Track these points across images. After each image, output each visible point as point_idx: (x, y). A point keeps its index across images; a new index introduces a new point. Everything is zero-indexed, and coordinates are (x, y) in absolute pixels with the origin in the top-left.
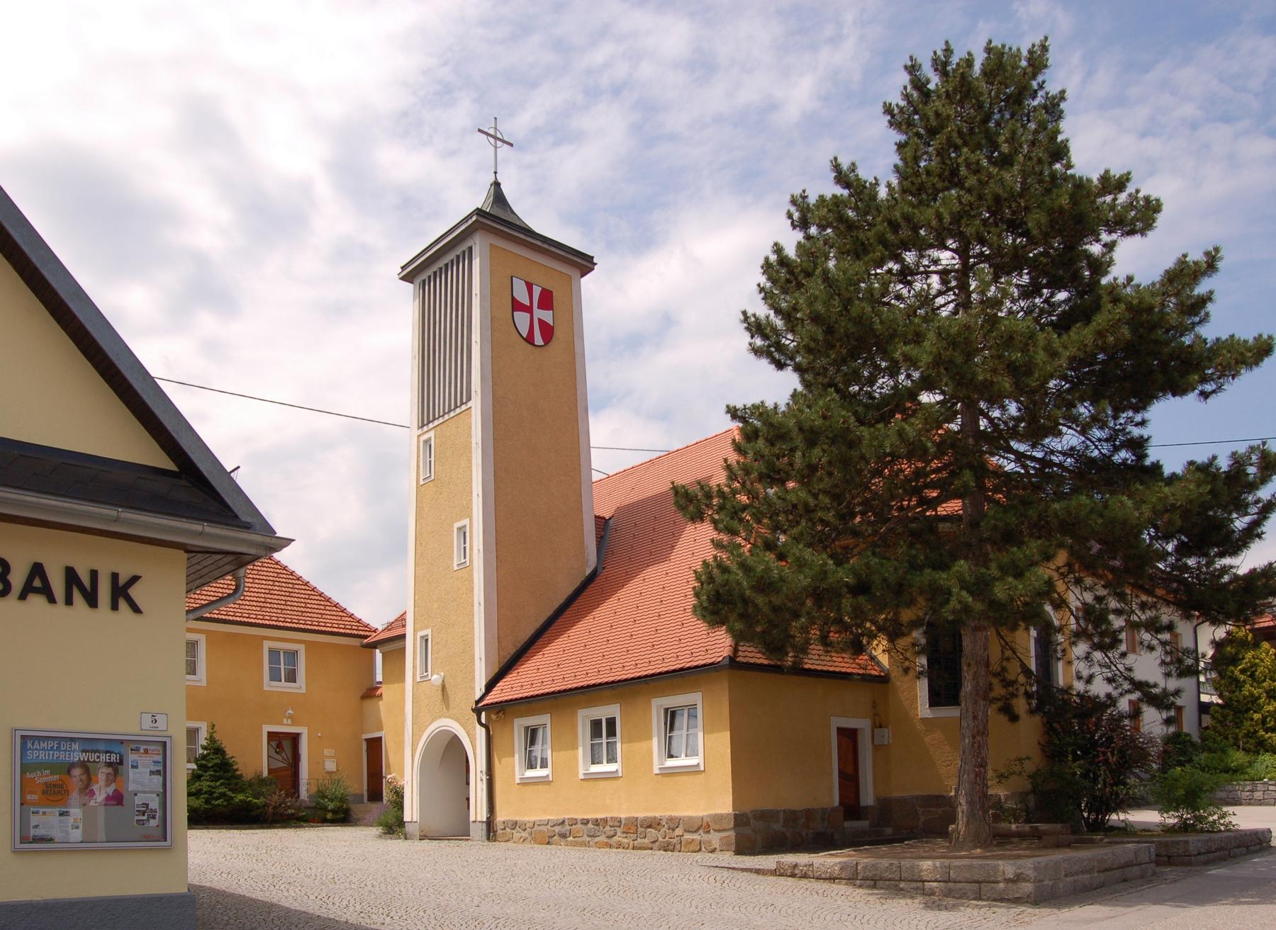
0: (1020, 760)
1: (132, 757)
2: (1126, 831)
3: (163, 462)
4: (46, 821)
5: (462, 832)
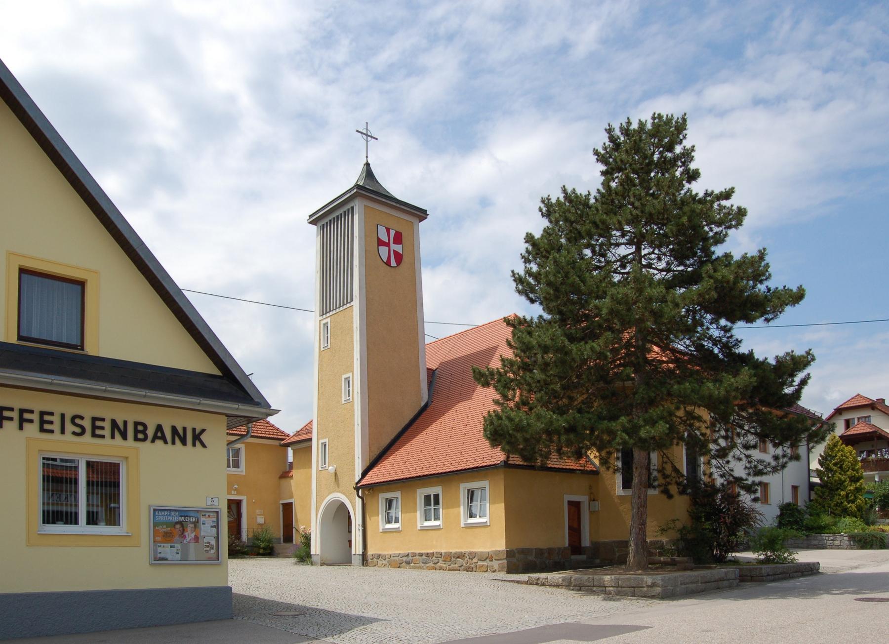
1: (202, 519)
4: (166, 550)
5: (346, 561)
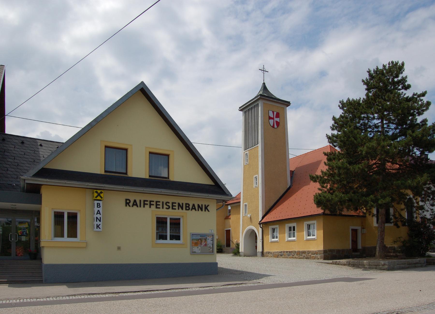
0: (400, 238)
1: (208, 238)
2: (429, 256)
3: (213, 184)
4: (196, 249)
5: (254, 254)
